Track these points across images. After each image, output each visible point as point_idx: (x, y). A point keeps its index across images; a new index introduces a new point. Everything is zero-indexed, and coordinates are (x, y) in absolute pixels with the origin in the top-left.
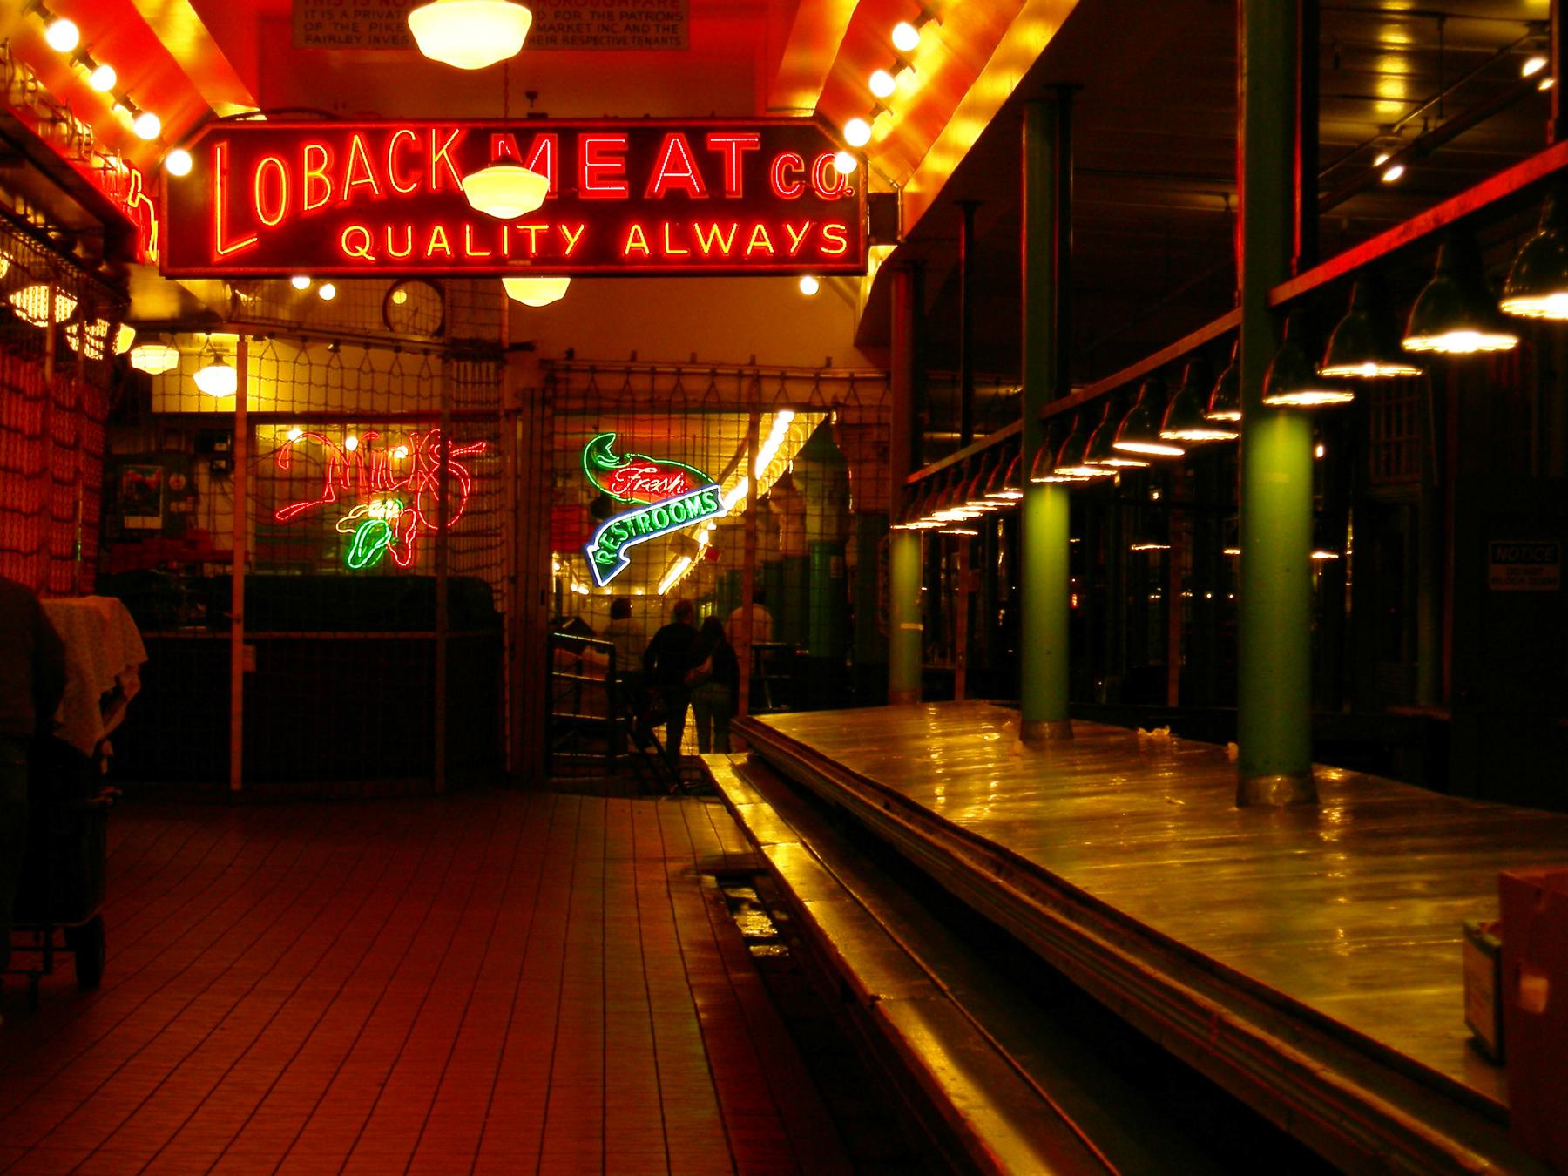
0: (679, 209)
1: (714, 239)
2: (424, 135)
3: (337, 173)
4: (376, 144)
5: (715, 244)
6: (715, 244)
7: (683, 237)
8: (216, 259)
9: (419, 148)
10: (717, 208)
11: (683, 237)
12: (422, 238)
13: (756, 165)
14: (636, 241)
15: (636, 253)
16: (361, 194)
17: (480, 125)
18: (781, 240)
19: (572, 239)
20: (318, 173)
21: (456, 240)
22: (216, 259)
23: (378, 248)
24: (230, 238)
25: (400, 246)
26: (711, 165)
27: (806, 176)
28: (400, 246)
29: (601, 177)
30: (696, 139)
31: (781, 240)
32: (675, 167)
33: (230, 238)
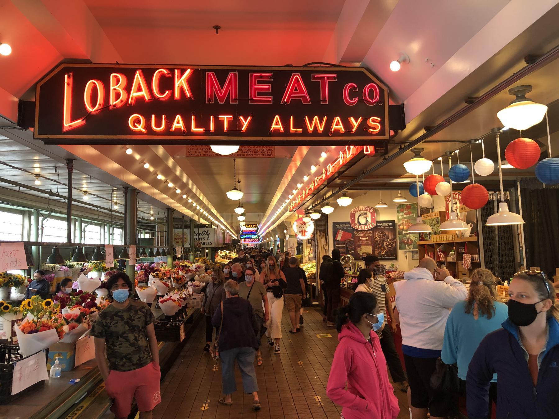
0: (298, 111)
1: (315, 124)
2: (172, 71)
3: (128, 89)
4: (148, 76)
5: (316, 128)
6: (316, 128)
7: (300, 123)
8: (65, 130)
9: (170, 75)
10: (316, 109)
11: (300, 123)
12: (170, 121)
13: (336, 89)
14: (277, 125)
15: (277, 132)
16: (140, 100)
17: (199, 68)
18: (347, 125)
19: (245, 123)
20: (116, 87)
21: (187, 124)
22: (65, 130)
23: (148, 126)
24: (73, 119)
25: (158, 125)
26: (313, 88)
27: (359, 94)
28: (158, 125)
29: (261, 93)
30: (306, 75)
31: (347, 125)
32: (295, 89)
33: (73, 119)
